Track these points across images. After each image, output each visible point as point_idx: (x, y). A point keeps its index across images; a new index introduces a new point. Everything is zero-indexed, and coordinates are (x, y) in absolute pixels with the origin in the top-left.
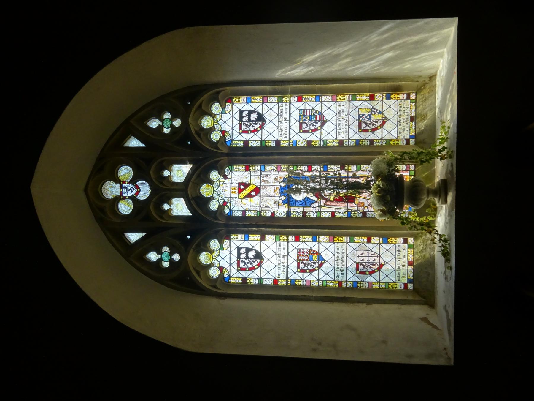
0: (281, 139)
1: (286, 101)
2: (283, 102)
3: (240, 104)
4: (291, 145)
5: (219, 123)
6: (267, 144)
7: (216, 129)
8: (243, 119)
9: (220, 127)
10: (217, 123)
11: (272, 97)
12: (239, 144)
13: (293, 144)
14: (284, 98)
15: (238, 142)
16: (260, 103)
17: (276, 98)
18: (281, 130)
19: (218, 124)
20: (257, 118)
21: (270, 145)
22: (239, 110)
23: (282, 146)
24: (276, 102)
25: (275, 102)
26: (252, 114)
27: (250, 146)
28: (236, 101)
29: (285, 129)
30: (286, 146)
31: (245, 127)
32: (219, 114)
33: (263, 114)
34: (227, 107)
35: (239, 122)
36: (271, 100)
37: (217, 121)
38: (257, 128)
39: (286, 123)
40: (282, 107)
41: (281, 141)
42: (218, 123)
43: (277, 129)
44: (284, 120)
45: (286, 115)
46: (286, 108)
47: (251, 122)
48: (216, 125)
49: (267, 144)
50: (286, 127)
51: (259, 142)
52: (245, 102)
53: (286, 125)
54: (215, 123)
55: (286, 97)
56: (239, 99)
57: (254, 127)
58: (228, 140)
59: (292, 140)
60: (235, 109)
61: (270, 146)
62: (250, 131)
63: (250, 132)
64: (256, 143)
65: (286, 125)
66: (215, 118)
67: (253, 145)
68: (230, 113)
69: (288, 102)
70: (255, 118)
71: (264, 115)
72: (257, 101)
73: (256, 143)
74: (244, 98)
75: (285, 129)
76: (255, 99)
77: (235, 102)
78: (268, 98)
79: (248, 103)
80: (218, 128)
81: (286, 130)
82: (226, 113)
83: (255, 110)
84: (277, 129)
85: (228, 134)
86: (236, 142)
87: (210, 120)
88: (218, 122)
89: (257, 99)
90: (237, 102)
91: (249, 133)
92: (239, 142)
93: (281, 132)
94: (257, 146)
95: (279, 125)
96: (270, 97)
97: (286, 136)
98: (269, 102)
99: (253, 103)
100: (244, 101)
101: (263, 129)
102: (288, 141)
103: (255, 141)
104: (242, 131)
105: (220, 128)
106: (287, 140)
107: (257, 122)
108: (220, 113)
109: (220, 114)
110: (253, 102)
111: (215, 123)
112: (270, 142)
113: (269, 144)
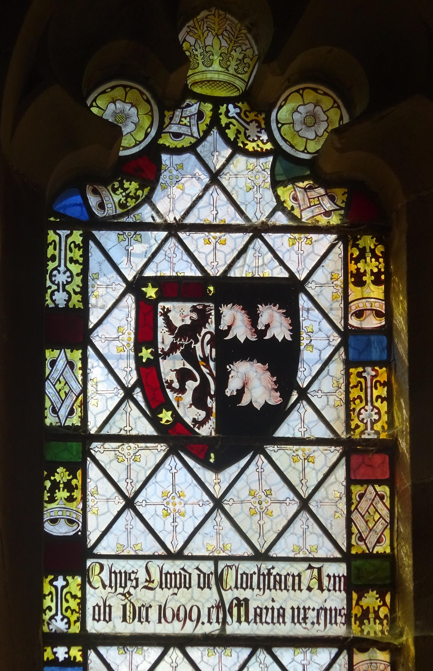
0: (95, 580)
1: (356, 611)
2: (355, 596)
3: (340, 282)
4: (48, 654)
5: (209, 139)
6: (57, 477)
7: (168, 114)
8: (237, 308)
9: (186, 142)
10: (207, 120)
11: (385, 512)
12: (61, 278)
13: (55, 662)
14: (378, 603)
15: (76, 269)
16: (348, 428)
17: (379, 541)
18: (156, 576)
19: (203, 127)
20: (245, 402)
21: (52, 500)
22: (301, 277)
23: (47, 588)
24: (349, 546)
25: (349, 534)
26: (272, 371)
27: (50, 354)
28: (357, 260)
29: (162, 611)
30: (46, 617)
31: (178, 324)
32: (272, 139)
33: (270, 449)
34: (321, 191)
35: (214, 280)
36: (364, 505)
37: (224, 121)
38: (170, 407)
39: (204, 618)
40: (321, 588)
41: (79, 579)
42: (209, 128)
43: (161, 552)
44: (228, 596)
45: (258, 615)
46: (312, 615)
47: (212, 364)
48: (200, 115)
49: (57, 477)
50: (176, 616)
51: (75, 420)
52: (354, 322)
53: (188, 616)
54: (208, 108)
55: (383, 612)
56: (377, 275)
57: (176, 385)
58: (93, 201)
59: (85, 656)
60: (307, 248)
61: (46, 496)
62: (155, 354)
63: (146, 354)
64: (68, 402)
65: (194, 616)
66: (244, 106)
67: (55, 375)
68: (279, 214)
69: (355, 627)
70: (241, 392)
71: (261, 459)
72: (358, 405)
73: (68, 402)
74: (378, 314)
75: (162, 611)
76: (376, 393)
77: (356, 253)
78: (381, 483)
79: (344, 343)
80: (174, 129)
81: (154, 614)
82: (280, 191)
83: (295, 396)
84: (161, 552)
85: (131, 203)
86: (77, 254)
87: (231, 71)
88: (215, 131)
89: (378, 404)
90: (352, 267)
91: (137, 349)
92: (78, 280)
93: (142, 576)
94: (48, 404)
95: (190, 566)
96: (387, 501)
97: (117, 613)
98: (356, 490)
99: (347, 375)
100: (359, 314)
101: (162, 448)
102: (75, 629)
103: (84, 390)
104: (155, 303)
105: (179, 144)
106: (83, 620)
107: (211, 403)
108: (282, 143)
109: (269, 146)
110: (353, 380)
111: (208, 108)
112: (70, 499)
113: (62, 494)
